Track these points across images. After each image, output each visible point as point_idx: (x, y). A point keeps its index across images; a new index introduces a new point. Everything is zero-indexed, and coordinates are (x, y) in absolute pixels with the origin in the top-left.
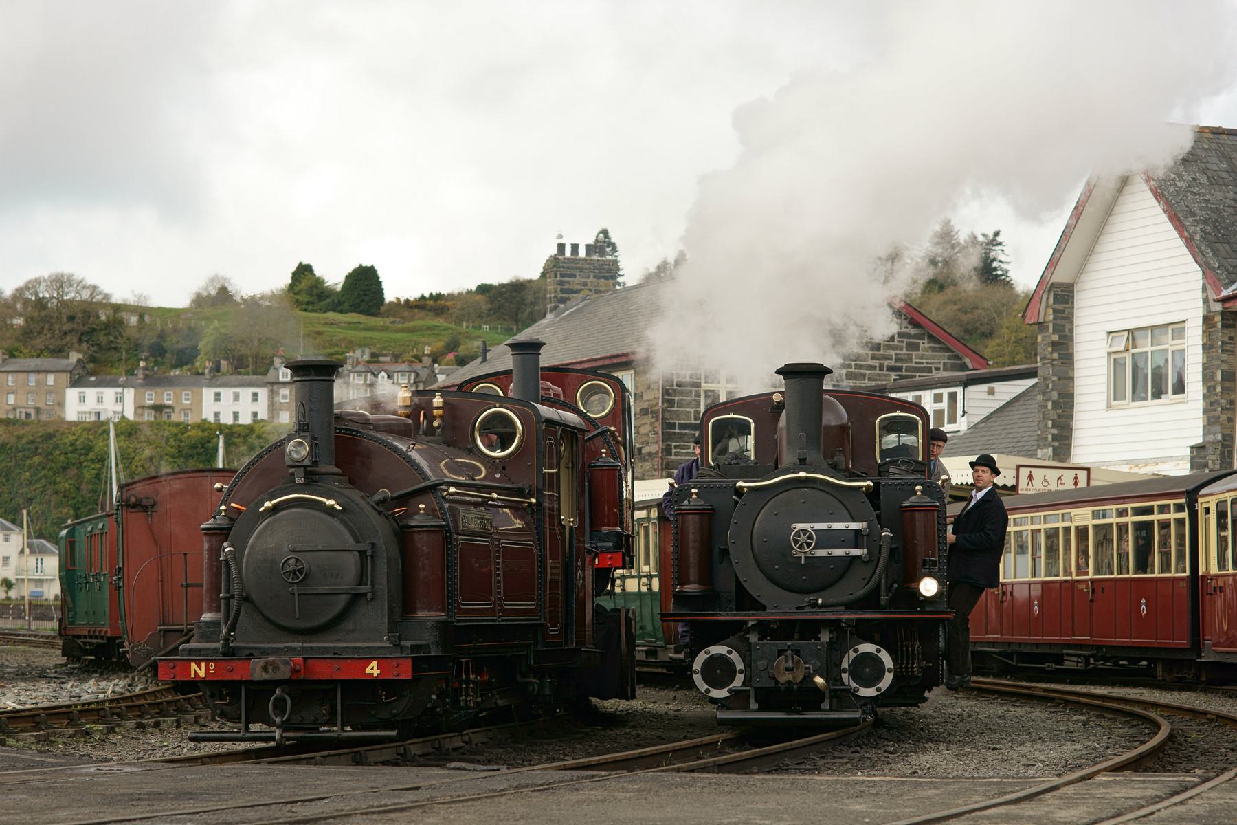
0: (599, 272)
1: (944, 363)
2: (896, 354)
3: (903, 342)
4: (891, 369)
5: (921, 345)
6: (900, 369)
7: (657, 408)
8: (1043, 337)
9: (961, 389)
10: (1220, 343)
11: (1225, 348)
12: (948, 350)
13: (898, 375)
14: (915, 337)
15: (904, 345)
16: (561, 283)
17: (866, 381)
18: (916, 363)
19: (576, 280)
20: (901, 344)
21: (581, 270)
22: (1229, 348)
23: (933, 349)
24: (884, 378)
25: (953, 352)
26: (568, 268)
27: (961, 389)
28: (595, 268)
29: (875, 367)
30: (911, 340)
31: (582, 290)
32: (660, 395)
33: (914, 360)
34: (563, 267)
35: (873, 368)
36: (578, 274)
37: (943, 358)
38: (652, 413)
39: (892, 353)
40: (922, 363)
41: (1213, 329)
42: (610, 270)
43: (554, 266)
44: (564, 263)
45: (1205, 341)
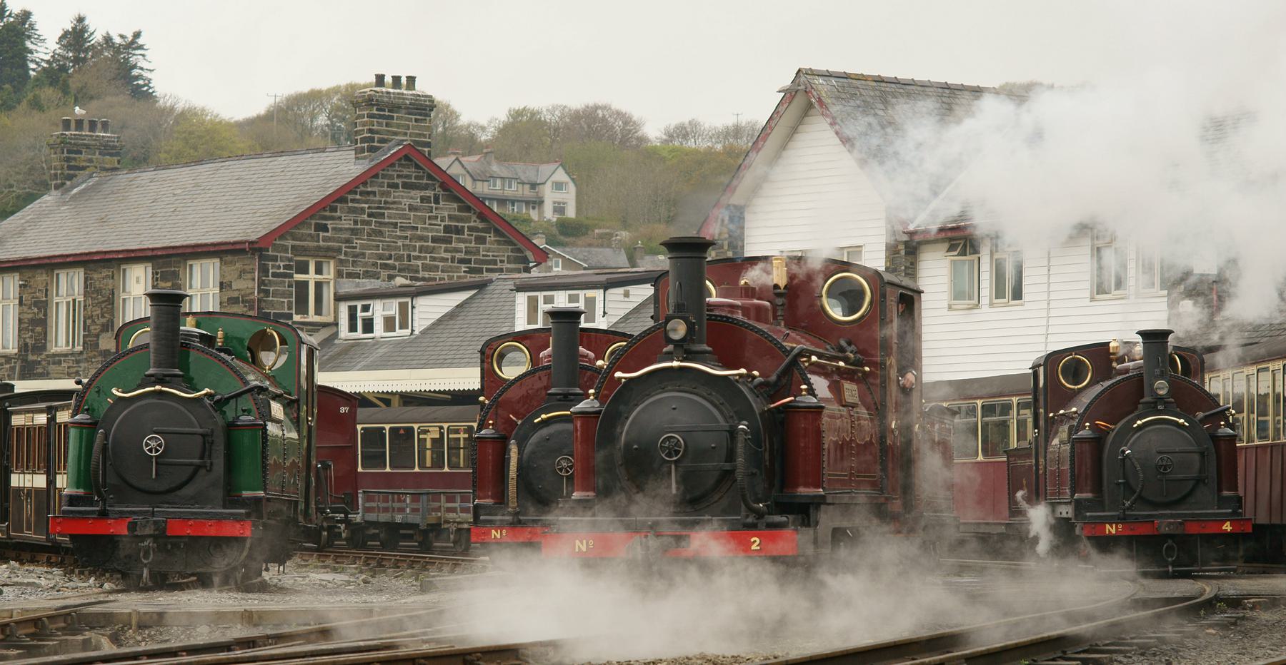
0: (105, 149)
1: (508, 256)
2: (466, 247)
3: (472, 235)
4: (461, 261)
5: (488, 238)
6: (469, 261)
7: (252, 297)
8: (717, 253)
9: (602, 291)
10: (903, 268)
11: (907, 272)
12: (510, 243)
13: (467, 267)
14: (483, 230)
15: (473, 238)
16: (68, 160)
17: (440, 273)
18: (483, 255)
19: (83, 156)
20: (470, 237)
21: (87, 146)
22: (910, 272)
23: (499, 242)
24: (455, 270)
25: (515, 245)
26: (74, 144)
27: (602, 291)
28: (101, 145)
29: (448, 259)
30: (479, 234)
31: (88, 167)
32: (256, 285)
33: (482, 253)
34: (70, 143)
35: (445, 260)
36: (84, 150)
37: (506, 252)
38: (243, 302)
39: (462, 246)
40: (489, 256)
41: (897, 255)
42: (116, 146)
43: (62, 142)
44: (71, 139)
45: (888, 265)
